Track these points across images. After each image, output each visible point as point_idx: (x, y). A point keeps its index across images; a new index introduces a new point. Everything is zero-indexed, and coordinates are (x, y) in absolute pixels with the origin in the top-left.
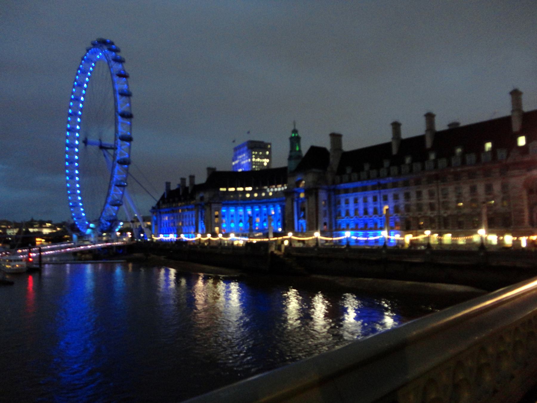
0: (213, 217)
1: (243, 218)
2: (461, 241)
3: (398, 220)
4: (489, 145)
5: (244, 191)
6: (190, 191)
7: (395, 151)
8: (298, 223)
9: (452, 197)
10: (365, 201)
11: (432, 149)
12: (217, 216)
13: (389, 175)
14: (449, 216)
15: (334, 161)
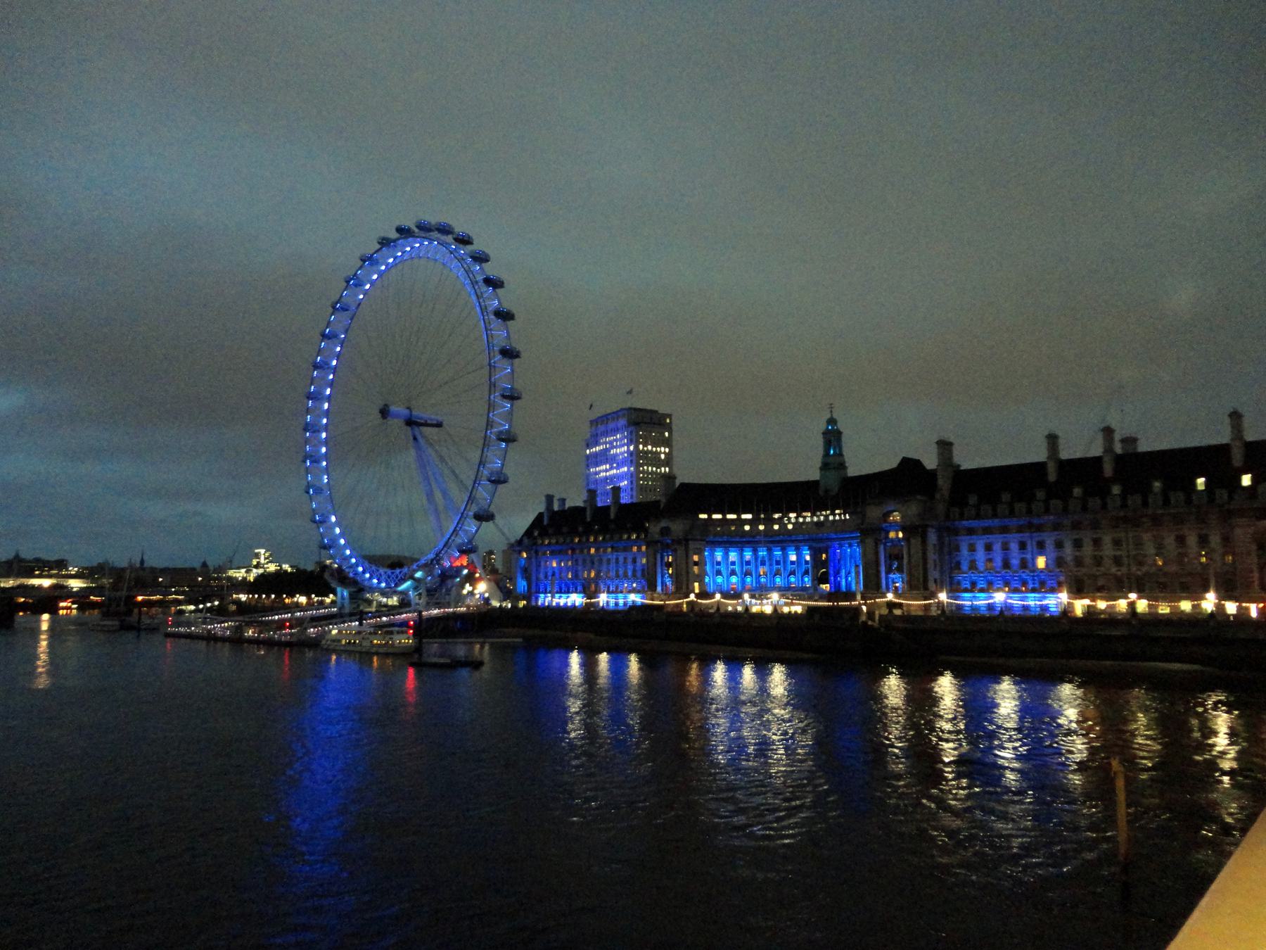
0: (691, 564)
1: (737, 568)
2: (1164, 609)
3: (1062, 578)
4: (1201, 482)
5: (739, 519)
6: (612, 516)
7: (1052, 476)
8: (887, 578)
9: (1150, 549)
10: (1005, 548)
11: (1113, 480)
12: (696, 564)
13: (1047, 511)
14: (1145, 575)
15: (944, 483)
